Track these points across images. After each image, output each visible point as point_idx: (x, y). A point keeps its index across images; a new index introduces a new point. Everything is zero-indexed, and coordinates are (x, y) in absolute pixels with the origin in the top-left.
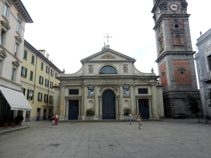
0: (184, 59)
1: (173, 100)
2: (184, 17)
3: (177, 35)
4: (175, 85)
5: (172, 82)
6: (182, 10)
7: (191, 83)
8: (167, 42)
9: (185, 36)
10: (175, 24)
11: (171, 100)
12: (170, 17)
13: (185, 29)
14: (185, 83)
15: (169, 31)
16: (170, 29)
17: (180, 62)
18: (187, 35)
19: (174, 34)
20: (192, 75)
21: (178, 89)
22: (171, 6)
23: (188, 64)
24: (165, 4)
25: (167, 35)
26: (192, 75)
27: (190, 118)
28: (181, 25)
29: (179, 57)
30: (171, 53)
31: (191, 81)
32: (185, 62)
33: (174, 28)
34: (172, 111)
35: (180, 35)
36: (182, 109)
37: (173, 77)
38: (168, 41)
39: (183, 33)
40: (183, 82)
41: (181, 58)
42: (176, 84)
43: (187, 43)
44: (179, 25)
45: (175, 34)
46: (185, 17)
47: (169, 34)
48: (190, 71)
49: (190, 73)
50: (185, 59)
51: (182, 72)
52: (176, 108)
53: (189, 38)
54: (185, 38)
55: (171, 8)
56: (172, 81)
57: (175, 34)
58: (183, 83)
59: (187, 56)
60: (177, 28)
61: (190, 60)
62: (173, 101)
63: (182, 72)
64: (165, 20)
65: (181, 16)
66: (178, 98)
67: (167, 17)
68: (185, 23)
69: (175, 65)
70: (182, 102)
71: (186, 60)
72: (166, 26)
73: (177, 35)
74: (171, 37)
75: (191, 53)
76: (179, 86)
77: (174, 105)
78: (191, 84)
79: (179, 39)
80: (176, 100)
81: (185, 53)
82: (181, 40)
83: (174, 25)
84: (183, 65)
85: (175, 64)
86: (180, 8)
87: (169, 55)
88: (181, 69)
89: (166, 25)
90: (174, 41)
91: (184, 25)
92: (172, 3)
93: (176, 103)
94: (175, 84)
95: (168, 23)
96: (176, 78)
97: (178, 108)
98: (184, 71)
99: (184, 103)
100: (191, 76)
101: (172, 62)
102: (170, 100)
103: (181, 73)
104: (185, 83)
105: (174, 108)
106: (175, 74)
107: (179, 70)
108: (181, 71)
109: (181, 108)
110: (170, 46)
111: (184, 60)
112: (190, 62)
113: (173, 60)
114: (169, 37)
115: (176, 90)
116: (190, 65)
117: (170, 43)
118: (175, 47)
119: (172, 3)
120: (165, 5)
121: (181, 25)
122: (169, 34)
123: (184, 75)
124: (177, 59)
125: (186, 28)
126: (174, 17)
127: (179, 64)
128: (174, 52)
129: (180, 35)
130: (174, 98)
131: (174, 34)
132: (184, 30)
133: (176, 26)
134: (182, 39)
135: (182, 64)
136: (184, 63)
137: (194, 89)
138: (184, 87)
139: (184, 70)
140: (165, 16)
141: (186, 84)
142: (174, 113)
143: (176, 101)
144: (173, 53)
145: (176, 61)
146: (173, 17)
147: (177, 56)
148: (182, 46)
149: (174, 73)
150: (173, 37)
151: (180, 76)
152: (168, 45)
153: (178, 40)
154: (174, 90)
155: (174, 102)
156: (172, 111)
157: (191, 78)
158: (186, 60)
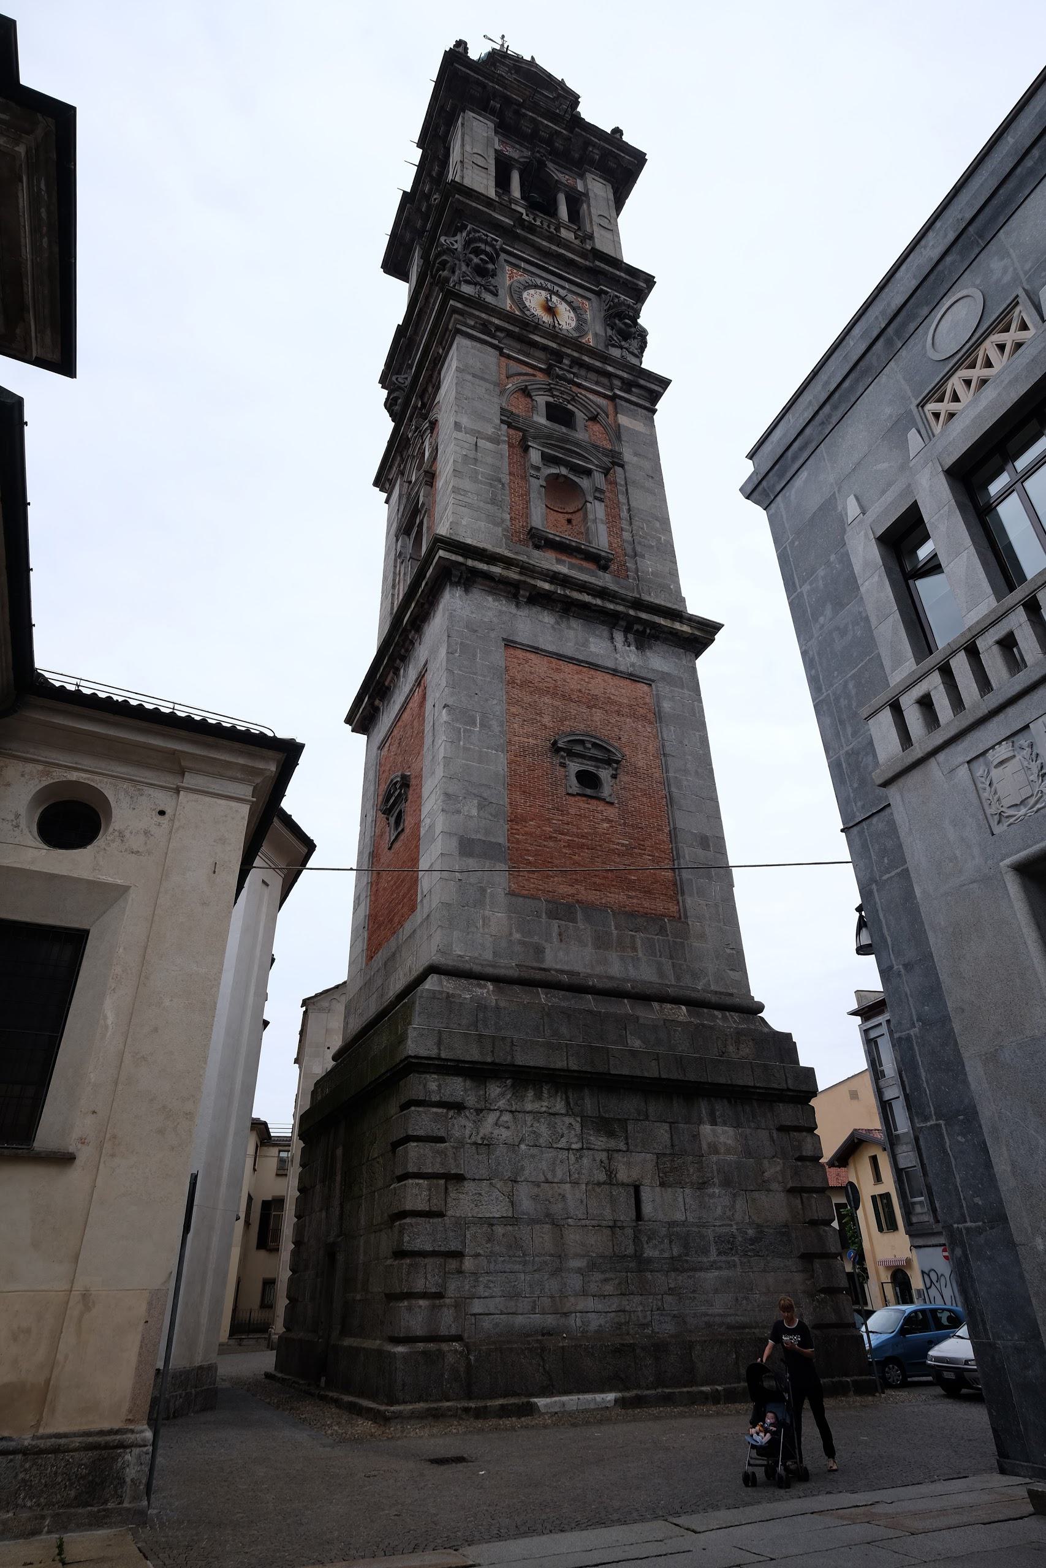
0: (610, 664)
1: (456, 1088)
2: (617, 383)
3: (564, 471)
4: (501, 898)
5: (472, 863)
6: (610, 342)
7: (674, 908)
8: (466, 484)
9: (622, 499)
10: (551, 399)
11: (433, 1085)
12: (510, 334)
13: (628, 456)
14: (616, 897)
15: (490, 421)
16: (503, 411)
17: (572, 678)
18: (639, 500)
19: (535, 456)
20: (681, 824)
21: (539, 951)
22: (525, 295)
23: (645, 717)
24: (483, 246)
25: (472, 439)
26: (688, 823)
27: (667, 1400)
28: (594, 419)
29: (571, 634)
30: (496, 570)
31: (676, 889)
32: (623, 691)
33: (541, 419)
34: (425, 1279)
35: (584, 483)
36: (572, 1237)
37: (481, 807)
38: (474, 479)
39: (606, 472)
40: (597, 888)
41: (586, 644)
42: (511, 894)
43: (639, 549)
44: (580, 416)
45: (543, 454)
46: (628, 386)
47: (495, 441)
48: (666, 783)
49: (671, 800)
50: (622, 668)
51: (588, 780)
52: (490, 1222)
53: (658, 525)
54: (624, 514)
55: (527, 304)
56: (467, 847)
57: (548, 459)
58: (592, 896)
59: (640, 647)
60: (564, 429)
61: (663, 689)
62: (458, 1107)
63: (588, 780)
64: (466, 342)
65: (598, 364)
66: (521, 1060)
67: (485, 328)
68: (623, 420)
69: (516, 692)
70: (570, 1130)
71: (632, 678)
72: (469, 377)
73: (564, 471)
74: (505, 468)
75: (677, 626)
76: (553, 915)
77: (460, 1178)
78: (681, 918)
79: (577, 518)
80: (494, 1090)
81: (620, 608)
82: (591, 516)
83: (541, 400)
84: (598, 715)
85: (525, 684)
86: (596, 335)
87: (467, 591)
88: (578, 748)
89: (474, 376)
90: (528, 502)
91: (617, 433)
92: (539, 281)
93: (487, 1145)
94: (500, 892)
95: (494, 368)
96: (515, 820)
97: (512, 1221)
98: (604, 774)
99: (600, 1142)
100: (673, 834)
101: (498, 656)
102: (418, 1093)
103: (574, 780)
104: (616, 897)
105: (462, 1224)
106: (516, 783)
107: (555, 749)
108: (574, 767)
109: (556, 1224)
110: (496, 524)
111: (615, 672)
112: (666, 706)
113: (509, 644)
114: (489, 460)
115: (508, 966)
116: (670, 733)
117: (493, 501)
118: (537, 547)
119: (539, 281)
120: (477, 252)
121: (596, 428)
122: (490, 439)
123: (611, 812)
124: (547, 642)
125: (636, 454)
126: (545, 348)
127: (566, 698)
128: (526, 569)
129: (584, 483)
130: (473, 1054)
131: (535, 456)
132: (616, 461)
133: (559, 414)
134: (597, 510)
135: (592, 702)
136: (610, 701)
137: (706, 984)
138: (602, 942)
139: (609, 762)
140: (477, 313)
141: (632, 915)
142: (447, 1322)
143: (491, 1118)
144: (513, 575)
145: (539, 666)
146: (534, 345)
147: (548, 618)
148: (600, 561)
149: (500, 764)
150: (521, 472)
151: (561, 810)
152: (467, 505)
153: (569, 521)
154: (488, 956)
155: (462, 1127)
156: (425, 1279)
157: (675, 855)
158: (632, 678)
